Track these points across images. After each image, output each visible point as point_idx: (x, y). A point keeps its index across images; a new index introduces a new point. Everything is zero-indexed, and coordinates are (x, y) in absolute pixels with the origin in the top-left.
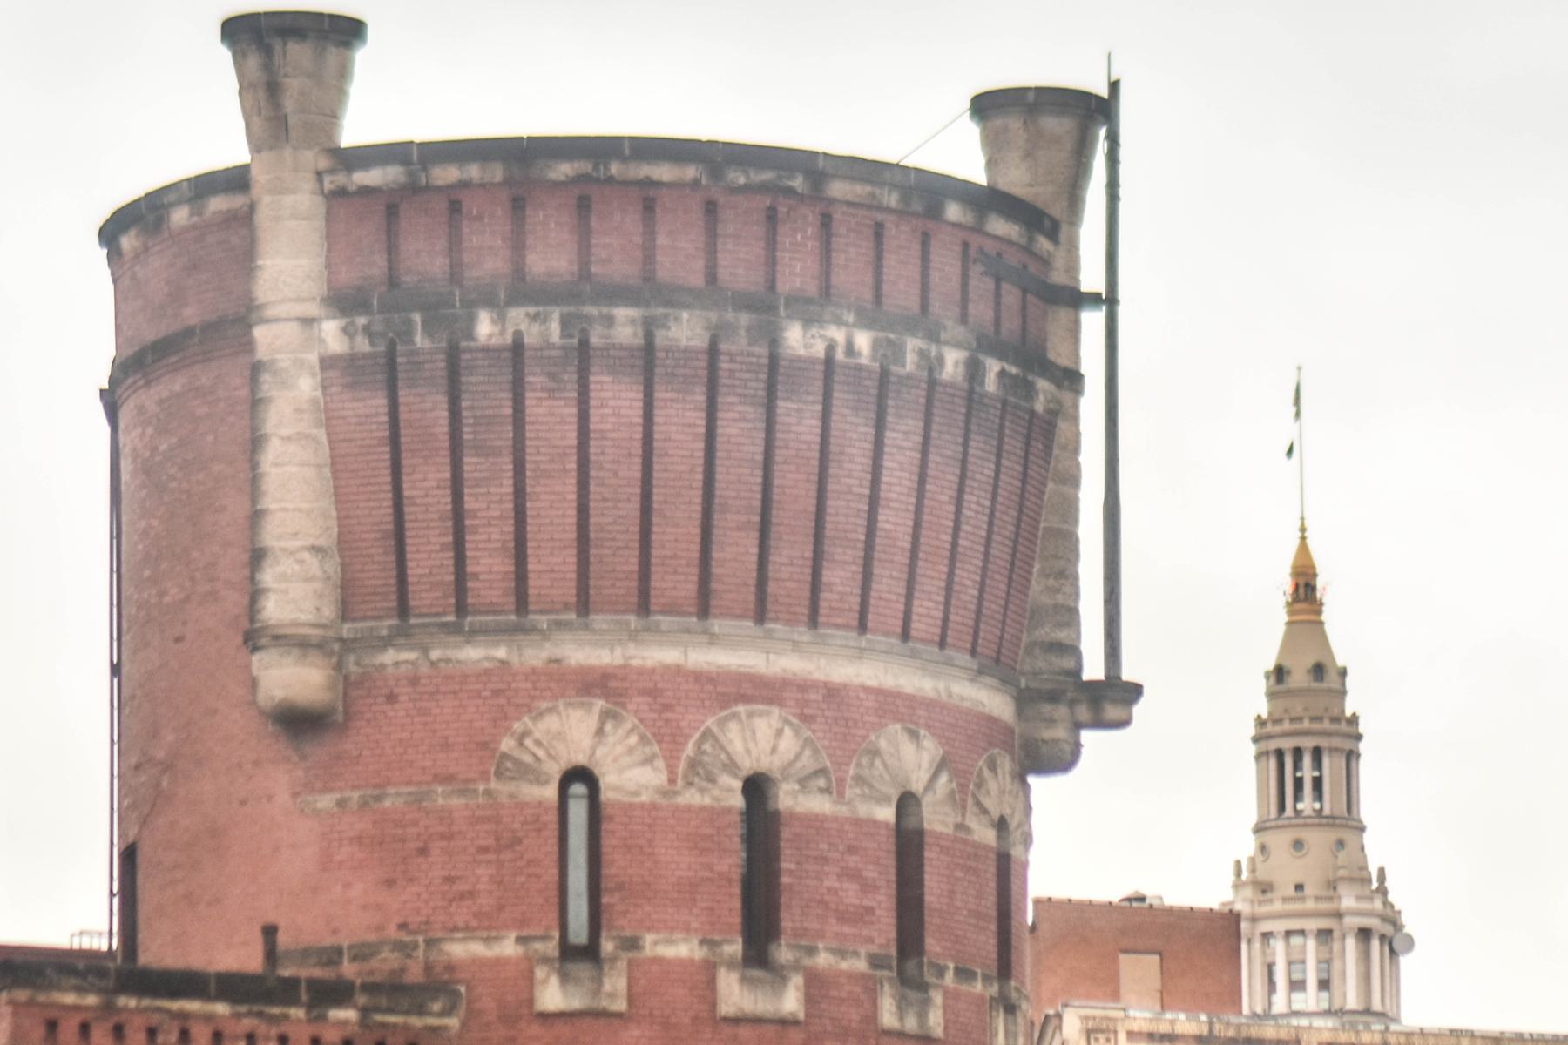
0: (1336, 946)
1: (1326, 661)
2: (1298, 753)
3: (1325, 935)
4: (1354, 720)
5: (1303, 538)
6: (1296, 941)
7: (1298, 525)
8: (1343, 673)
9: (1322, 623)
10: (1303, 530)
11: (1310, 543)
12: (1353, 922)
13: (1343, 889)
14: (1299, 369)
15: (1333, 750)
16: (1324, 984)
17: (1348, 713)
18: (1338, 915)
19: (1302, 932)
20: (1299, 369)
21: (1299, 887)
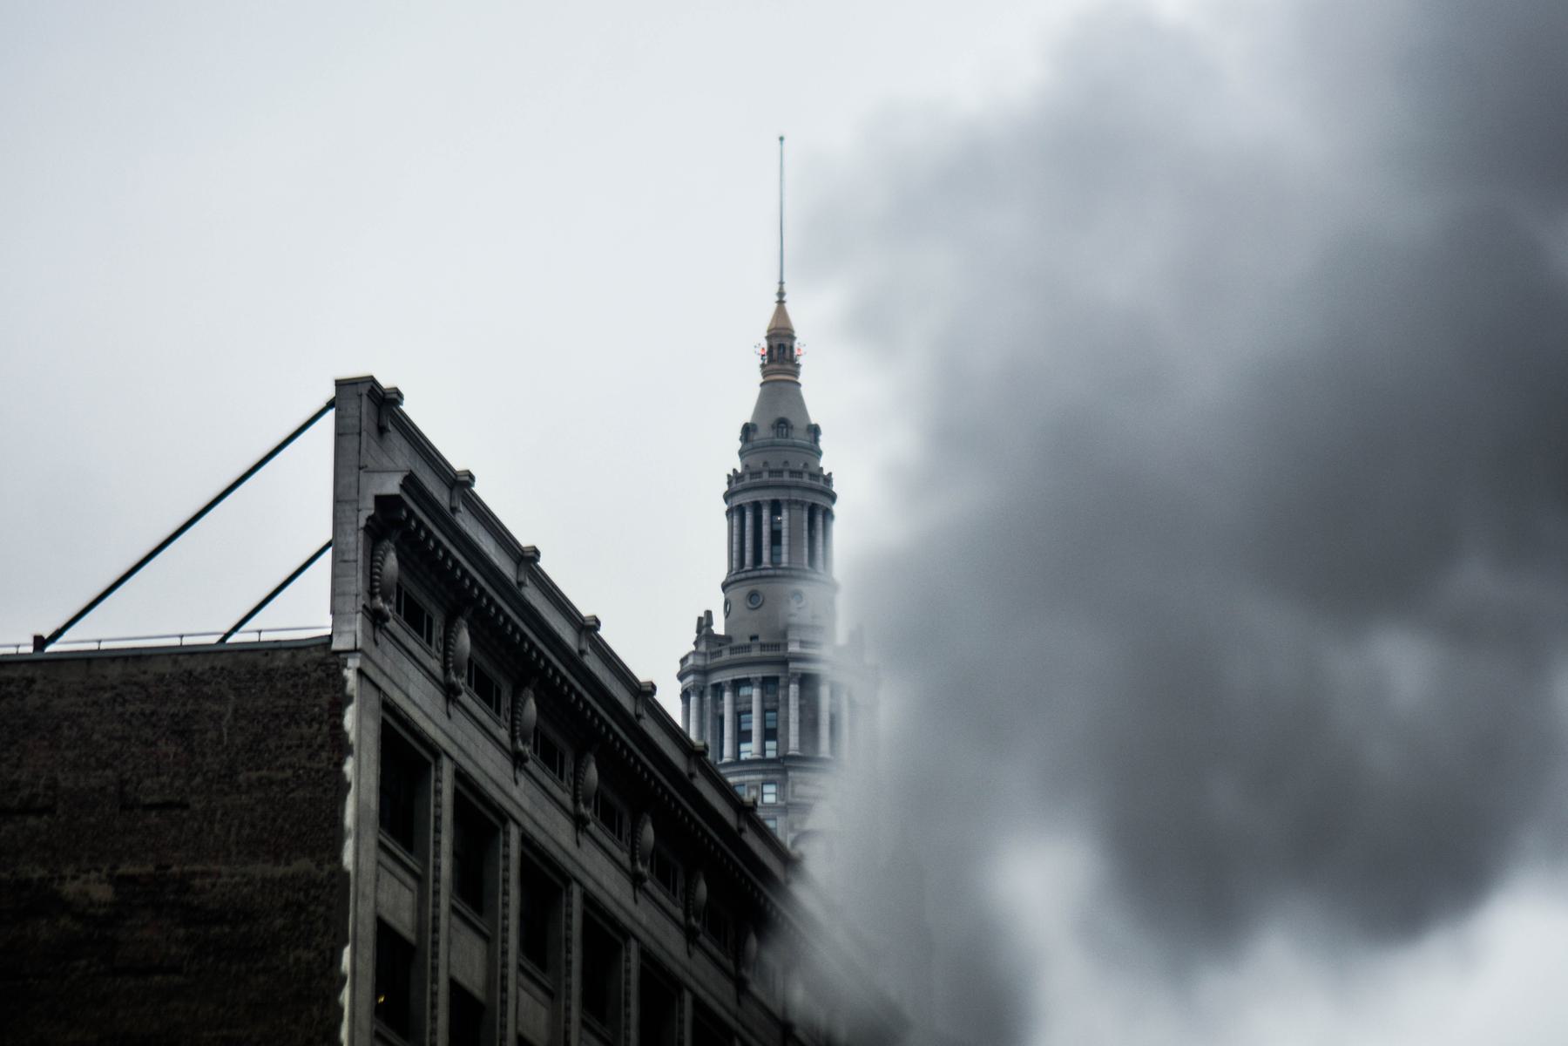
0: (781, 693)
1: (792, 419)
2: (757, 507)
3: (768, 684)
4: (828, 479)
6: (744, 691)
8: (815, 431)
11: (788, 306)
15: (791, 503)
16: (769, 734)
18: (784, 662)
19: (747, 682)
21: (754, 638)
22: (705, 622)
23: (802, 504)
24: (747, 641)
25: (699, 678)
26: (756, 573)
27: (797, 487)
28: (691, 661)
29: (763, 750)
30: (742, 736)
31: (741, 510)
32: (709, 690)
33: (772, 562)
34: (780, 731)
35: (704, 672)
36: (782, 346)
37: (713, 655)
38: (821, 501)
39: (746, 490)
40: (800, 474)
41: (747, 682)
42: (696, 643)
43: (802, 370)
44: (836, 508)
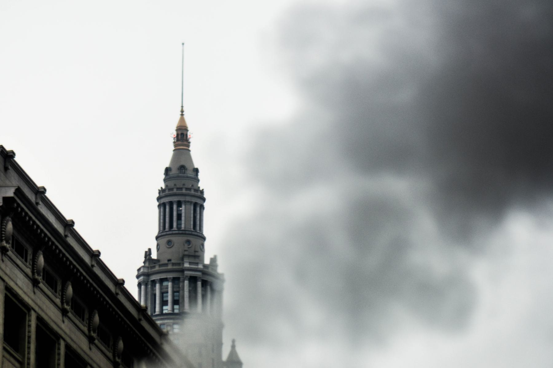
0: (181, 284)
1: (187, 166)
2: (171, 204)
3: (175, 280)
4: (202, 192)
5: (182, 115)
6: (165, 284)
7: (180, 109)
8: (196, 171)
9: (189, 151)
10: (182, 111)
11: (186, 117)
12: (187, 273)
13: (186, 260)
14: (183, 44)
15: (186, 202)
16: (176, 302)
17: (201, 189)
18: (182, 271)
19: (166, 279)
20: (183, 44)
21: (169, 260)
22: (148, 254)
23: (191, 202)
24: (166, 262)
25: (145, 277)
26: (171, 232)
28: (142, 270)
29: (173, 309)
30: (164, 303)
32: (150, 283)
33: (177, 227)
34: (180, 301)
35: (147, 275)
36: (182, 134)
38: (199, 201)
39: (166, 196)
40: (189, 189)
41: (166, 279)
42: (144, 262)
43: (191, 144)
44: (205, 204)
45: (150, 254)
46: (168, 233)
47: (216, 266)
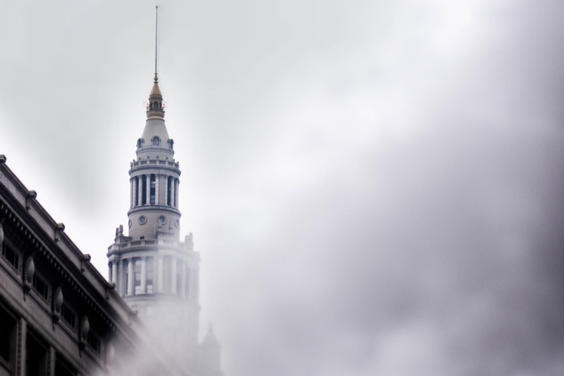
1: (161, 137)
2: (144, 177)
4: (177, 165)
5: (156, 83)
6: (138, 263)
7: (154, 76)
8: (171, 142)
10: (156, 79)
14: (157, 7)
17: (176, 162)
20: (157, 7)
21: (142, 238)
22: (119, 231)
23: (165, 176)
24: (139, 239)
25: (116, 256)
26: (143, 208)
27: (162, 168)
28: (113, 249)
29: (146, 290)
31: (137, 178)
32: (121, 262)
33: (151, 203)
34: (154, 280)
35: (119, 253)
37: (123, 245)
38: (174, 175)
39: (139, 169)
40: (163, 162)
41: (139, 258)
42: (116, 240)
43: (165, 114)
44: (181, 178)
45: (121, 232)
46: (140, 208)
47: (192, 244)
